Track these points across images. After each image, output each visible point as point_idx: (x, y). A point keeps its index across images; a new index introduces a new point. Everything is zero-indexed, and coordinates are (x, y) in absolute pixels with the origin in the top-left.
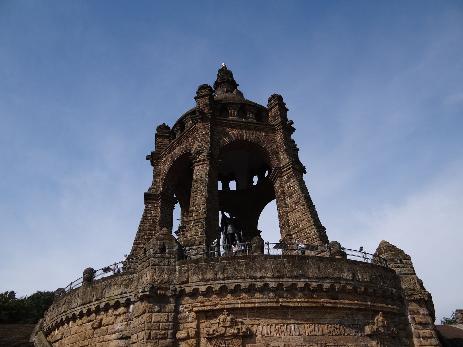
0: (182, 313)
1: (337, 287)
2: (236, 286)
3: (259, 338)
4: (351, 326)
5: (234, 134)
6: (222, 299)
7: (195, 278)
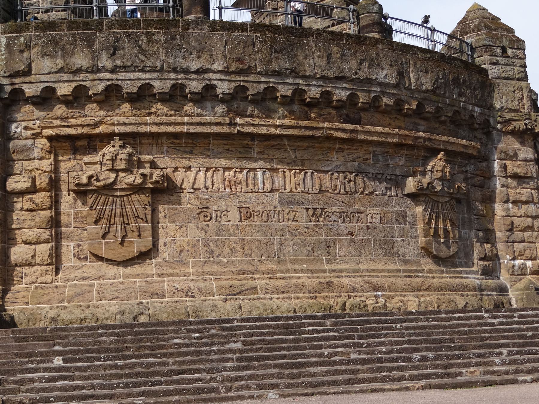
0: (18, 138)
1: (362, 98)
2: (141, 88)
3: (187, 195)
4: (380, 176)
6: (109, 114)
7: (47, 64)
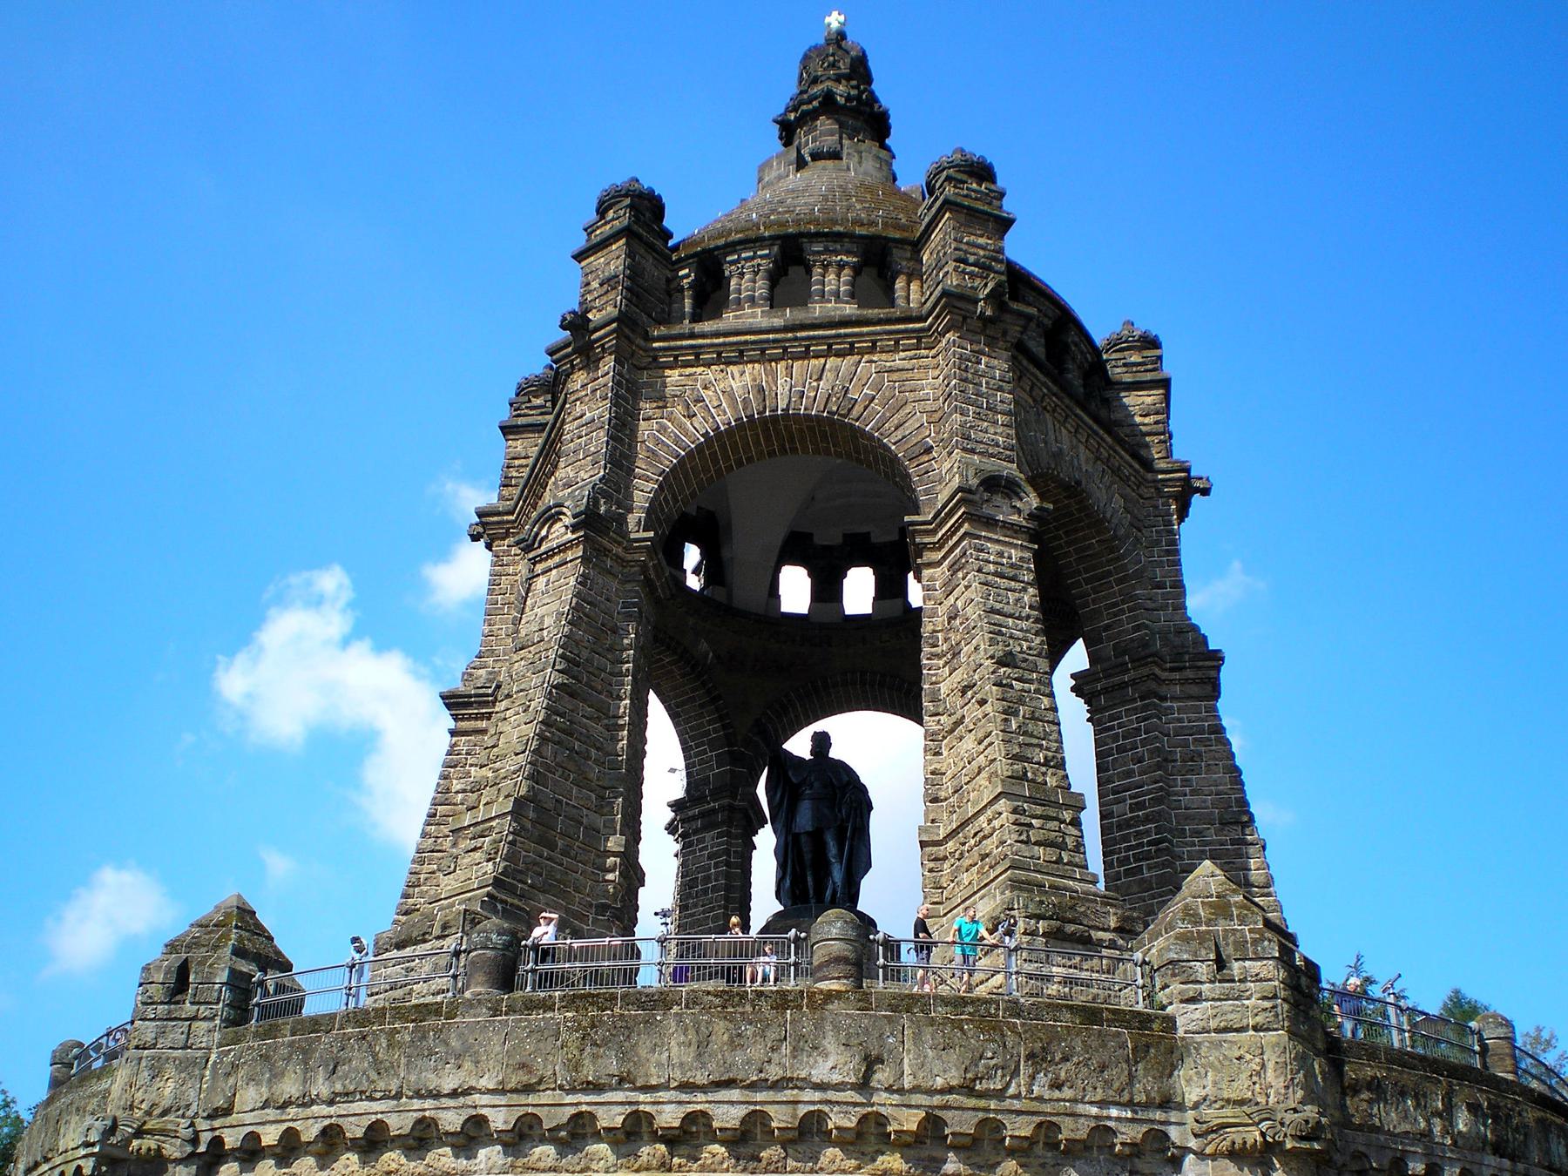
1: (780, 1118)
5: (730, 394)
